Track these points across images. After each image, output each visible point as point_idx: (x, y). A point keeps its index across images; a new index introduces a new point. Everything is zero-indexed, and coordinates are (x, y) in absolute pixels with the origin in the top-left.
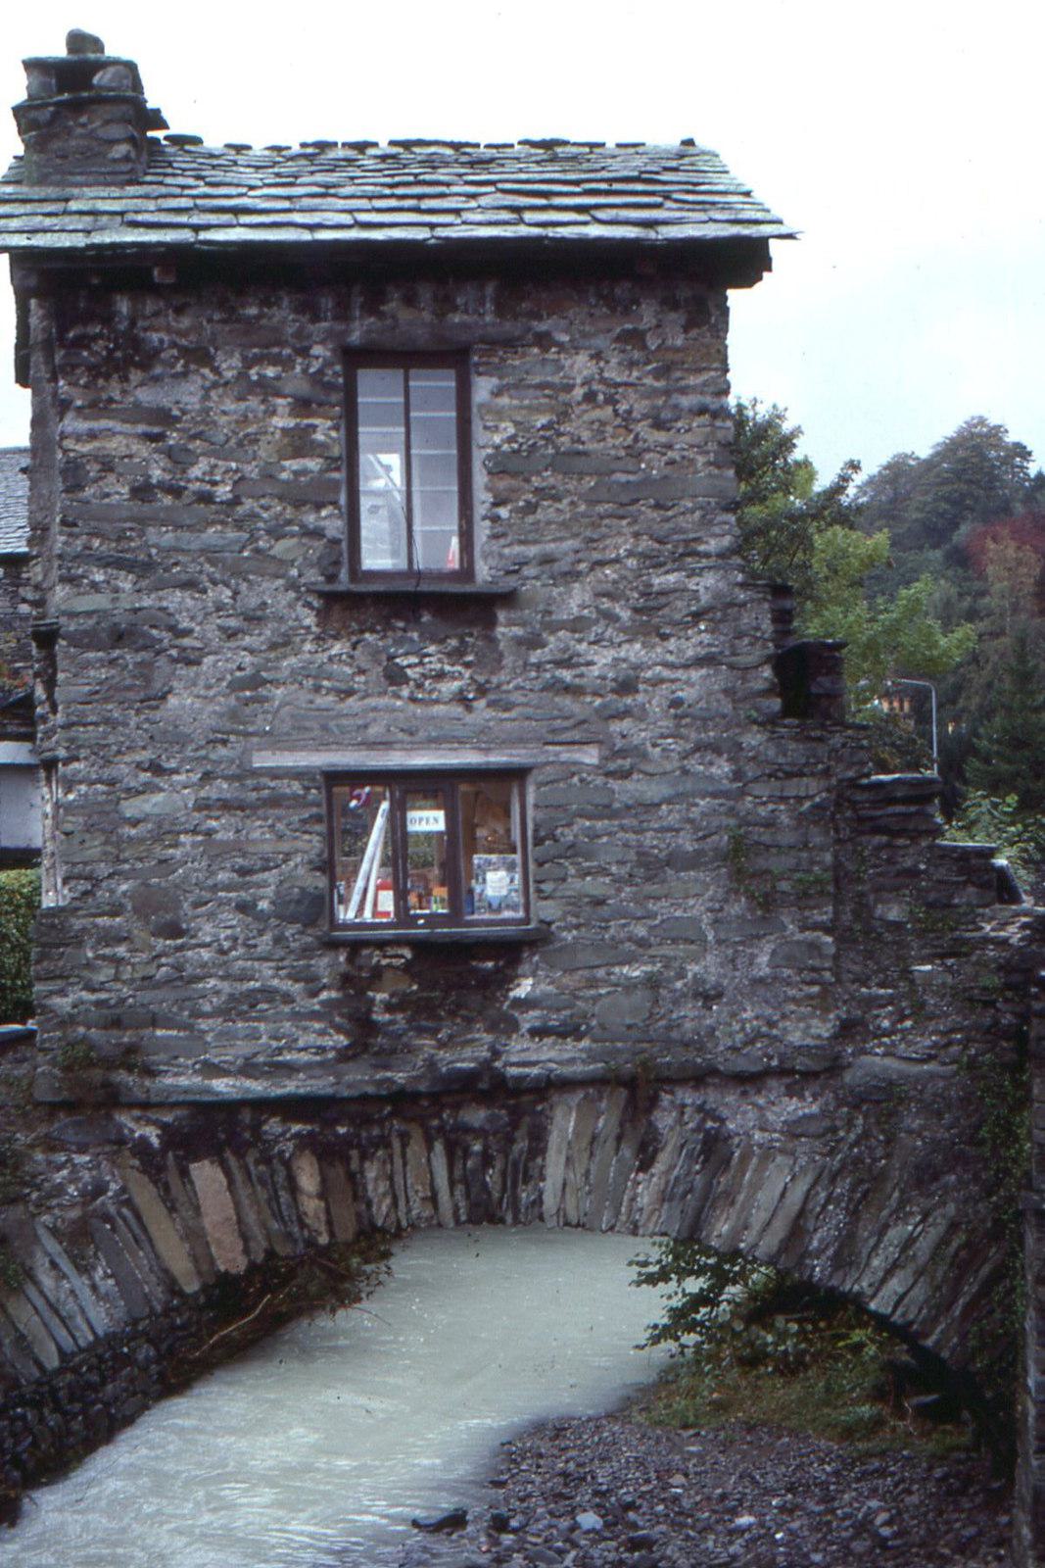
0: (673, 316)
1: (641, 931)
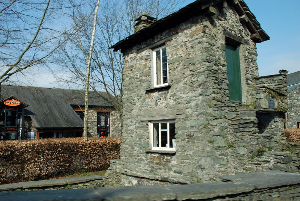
0: (193, 25)
1: (191, 152)
